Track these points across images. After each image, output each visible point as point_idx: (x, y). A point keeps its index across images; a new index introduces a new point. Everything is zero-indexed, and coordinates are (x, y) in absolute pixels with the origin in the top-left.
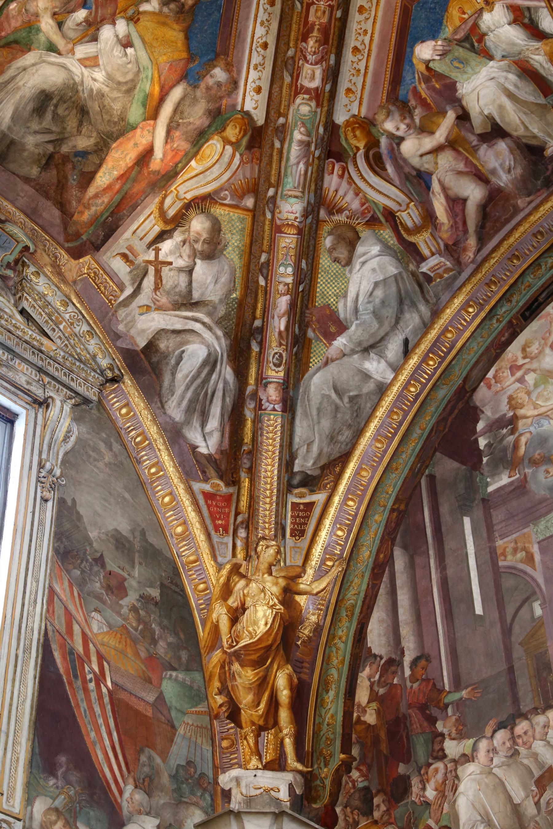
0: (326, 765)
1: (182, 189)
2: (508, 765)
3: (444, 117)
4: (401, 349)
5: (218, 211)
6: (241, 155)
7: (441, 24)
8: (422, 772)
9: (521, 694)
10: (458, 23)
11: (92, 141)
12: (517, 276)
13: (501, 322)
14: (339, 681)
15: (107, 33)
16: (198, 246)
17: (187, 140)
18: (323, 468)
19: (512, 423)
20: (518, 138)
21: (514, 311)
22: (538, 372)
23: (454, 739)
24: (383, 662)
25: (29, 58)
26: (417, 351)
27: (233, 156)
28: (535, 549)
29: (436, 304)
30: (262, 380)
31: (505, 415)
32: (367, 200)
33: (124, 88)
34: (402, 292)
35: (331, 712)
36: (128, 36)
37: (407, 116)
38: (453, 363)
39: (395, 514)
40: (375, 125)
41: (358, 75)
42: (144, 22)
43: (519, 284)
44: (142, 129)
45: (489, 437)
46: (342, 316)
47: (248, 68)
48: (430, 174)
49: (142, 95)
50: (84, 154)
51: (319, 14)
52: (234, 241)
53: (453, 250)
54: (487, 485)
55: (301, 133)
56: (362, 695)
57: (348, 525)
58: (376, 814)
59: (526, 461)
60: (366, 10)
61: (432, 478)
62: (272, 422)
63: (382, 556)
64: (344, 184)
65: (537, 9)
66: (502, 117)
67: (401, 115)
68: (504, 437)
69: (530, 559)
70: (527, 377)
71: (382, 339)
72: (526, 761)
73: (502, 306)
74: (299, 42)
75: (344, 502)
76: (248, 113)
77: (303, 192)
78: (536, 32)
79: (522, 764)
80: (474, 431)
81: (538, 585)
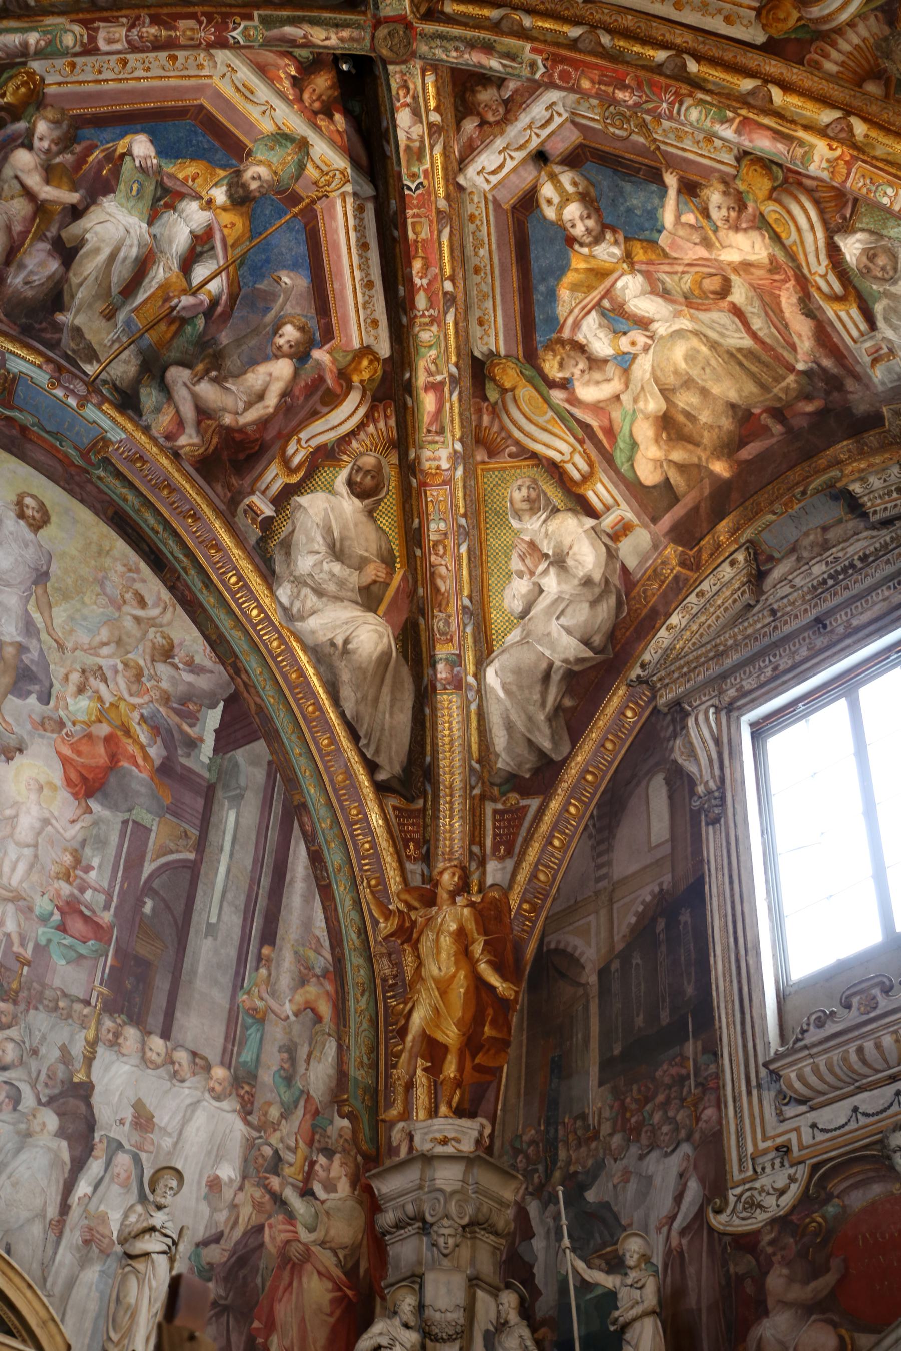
7: (177, 158)
10: (181, 176)
40: (37, 109)
51: (189, 33)
66: (87, 255)
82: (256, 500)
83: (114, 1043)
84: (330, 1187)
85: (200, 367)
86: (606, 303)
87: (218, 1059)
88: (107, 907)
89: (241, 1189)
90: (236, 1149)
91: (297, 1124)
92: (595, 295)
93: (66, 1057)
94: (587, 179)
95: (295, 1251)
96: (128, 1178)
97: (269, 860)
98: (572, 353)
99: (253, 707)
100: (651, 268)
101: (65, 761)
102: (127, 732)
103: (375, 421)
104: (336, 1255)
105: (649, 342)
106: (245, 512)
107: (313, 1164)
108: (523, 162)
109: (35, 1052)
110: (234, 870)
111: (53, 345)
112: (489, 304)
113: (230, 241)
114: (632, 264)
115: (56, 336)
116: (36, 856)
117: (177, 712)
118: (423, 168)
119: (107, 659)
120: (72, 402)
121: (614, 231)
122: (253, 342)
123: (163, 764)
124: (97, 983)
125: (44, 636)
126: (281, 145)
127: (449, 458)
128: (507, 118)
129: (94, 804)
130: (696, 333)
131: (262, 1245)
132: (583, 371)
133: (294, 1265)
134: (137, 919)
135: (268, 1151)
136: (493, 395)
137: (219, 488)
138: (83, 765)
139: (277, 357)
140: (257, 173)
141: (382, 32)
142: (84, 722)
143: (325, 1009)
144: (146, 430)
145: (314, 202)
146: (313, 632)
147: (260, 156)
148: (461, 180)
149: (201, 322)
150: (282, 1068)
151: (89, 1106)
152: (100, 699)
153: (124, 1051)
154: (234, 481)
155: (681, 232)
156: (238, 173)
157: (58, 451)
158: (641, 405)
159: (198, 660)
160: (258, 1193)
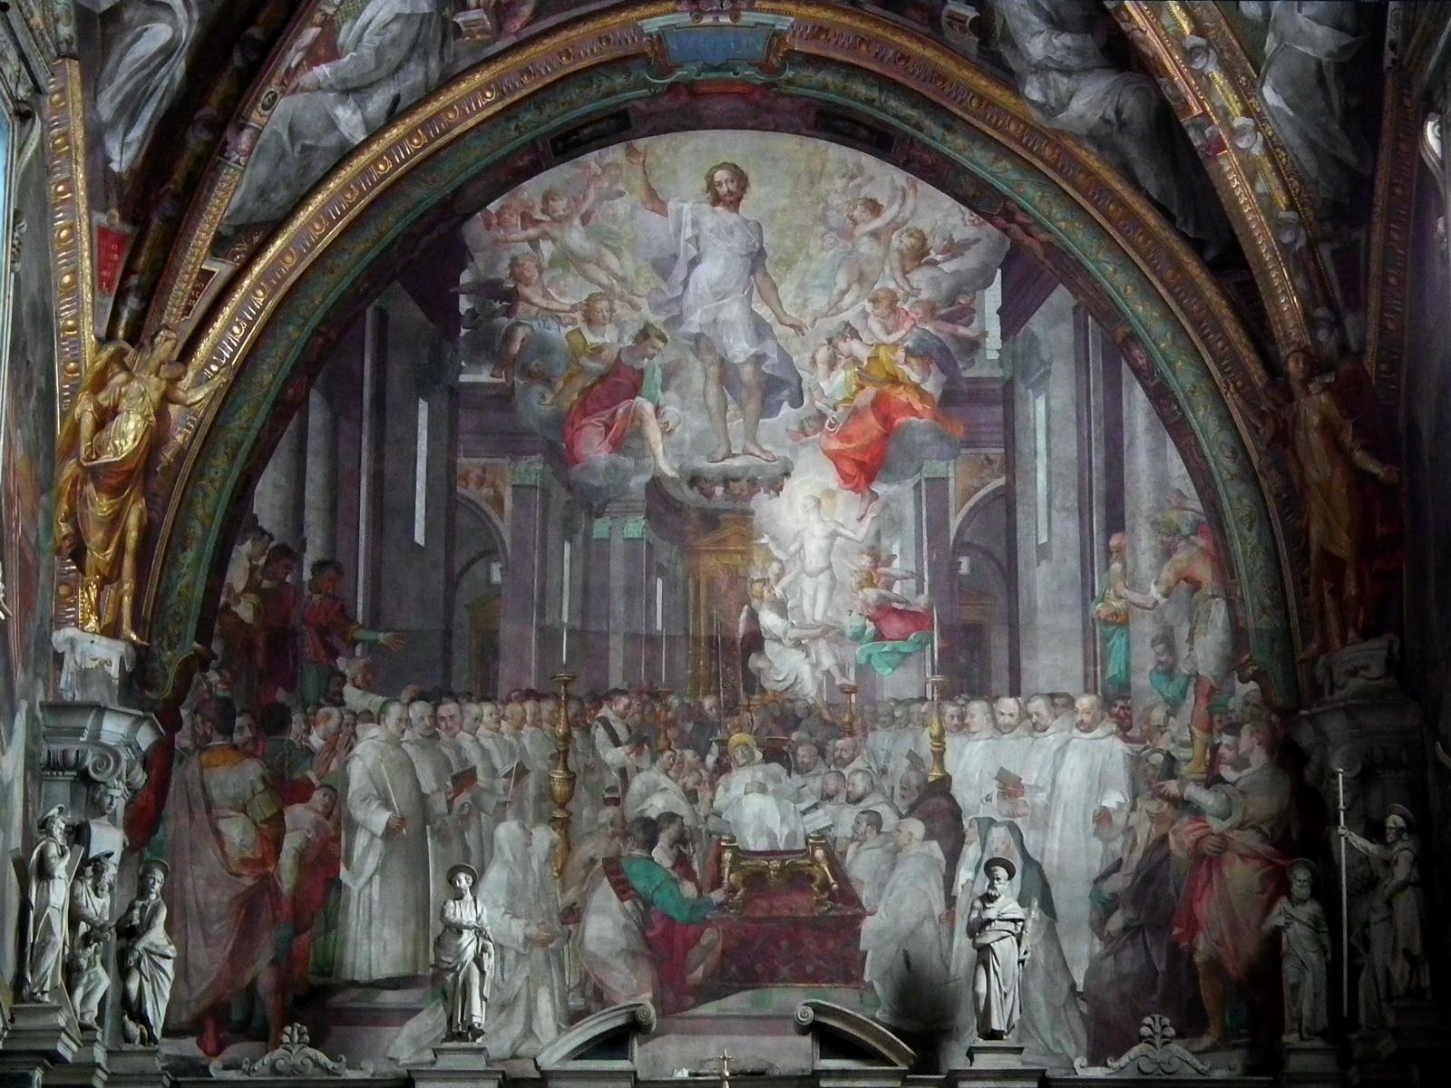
0: (171, 647)
2: (423, 747)
8: (309, 710)
9: (455, 668)
13: (521, 134)
14: (204, 540)
19: (512, 297)
21: (543, 129)
22: (558, 245)
23: (358, 687)
24: (273, 544)
28: (507, 493)
29: (450, 66)
35: (187, 579)
54: (460, 370)
56: (237, 576)
57: (247, 321)
58: (237, 737)
59: (518, 366)
61: (382, 316)
63: (290, 391)
68: (494, 314)
69: (498, 502)
72: (446, 751)
75: (252, 291)
79: (439, 750)
81: (502, 542)
83: (962, 726)
84: (1240, 763)
87: (1081, 689)
88: (919, 591)
89: (1133, 809)
90: (1120, 773)
91: (1189, 714)
93: (914, 757)
95: (1209, 846)
96: (1008, 847)
97: (1097, 431)
99: (1039, 250)
101: (835, 457)
102: (895, 380)
104: (1260, 830)
107: (1215, 749)
109: (884, 771)
110: (1054, 470)
116: (833, 578)
117: (950, 319)
119: (854, 307)
120: (725, 20)
123: (944, 394)
124: (928, 675)
125: (779, 329)
129: (880, 488)
131: (1168, 854)
133: (1211, 860)
134: (956, 586)
135: (1158, 758)
137: (912, 13)
138: (856, 450)
142: (845, 400)
143: (1204, 572)
150: (1159, 662)
151: (952, 799)
152: (856, 361)
153: (973, 729)
160: (1154, 806)
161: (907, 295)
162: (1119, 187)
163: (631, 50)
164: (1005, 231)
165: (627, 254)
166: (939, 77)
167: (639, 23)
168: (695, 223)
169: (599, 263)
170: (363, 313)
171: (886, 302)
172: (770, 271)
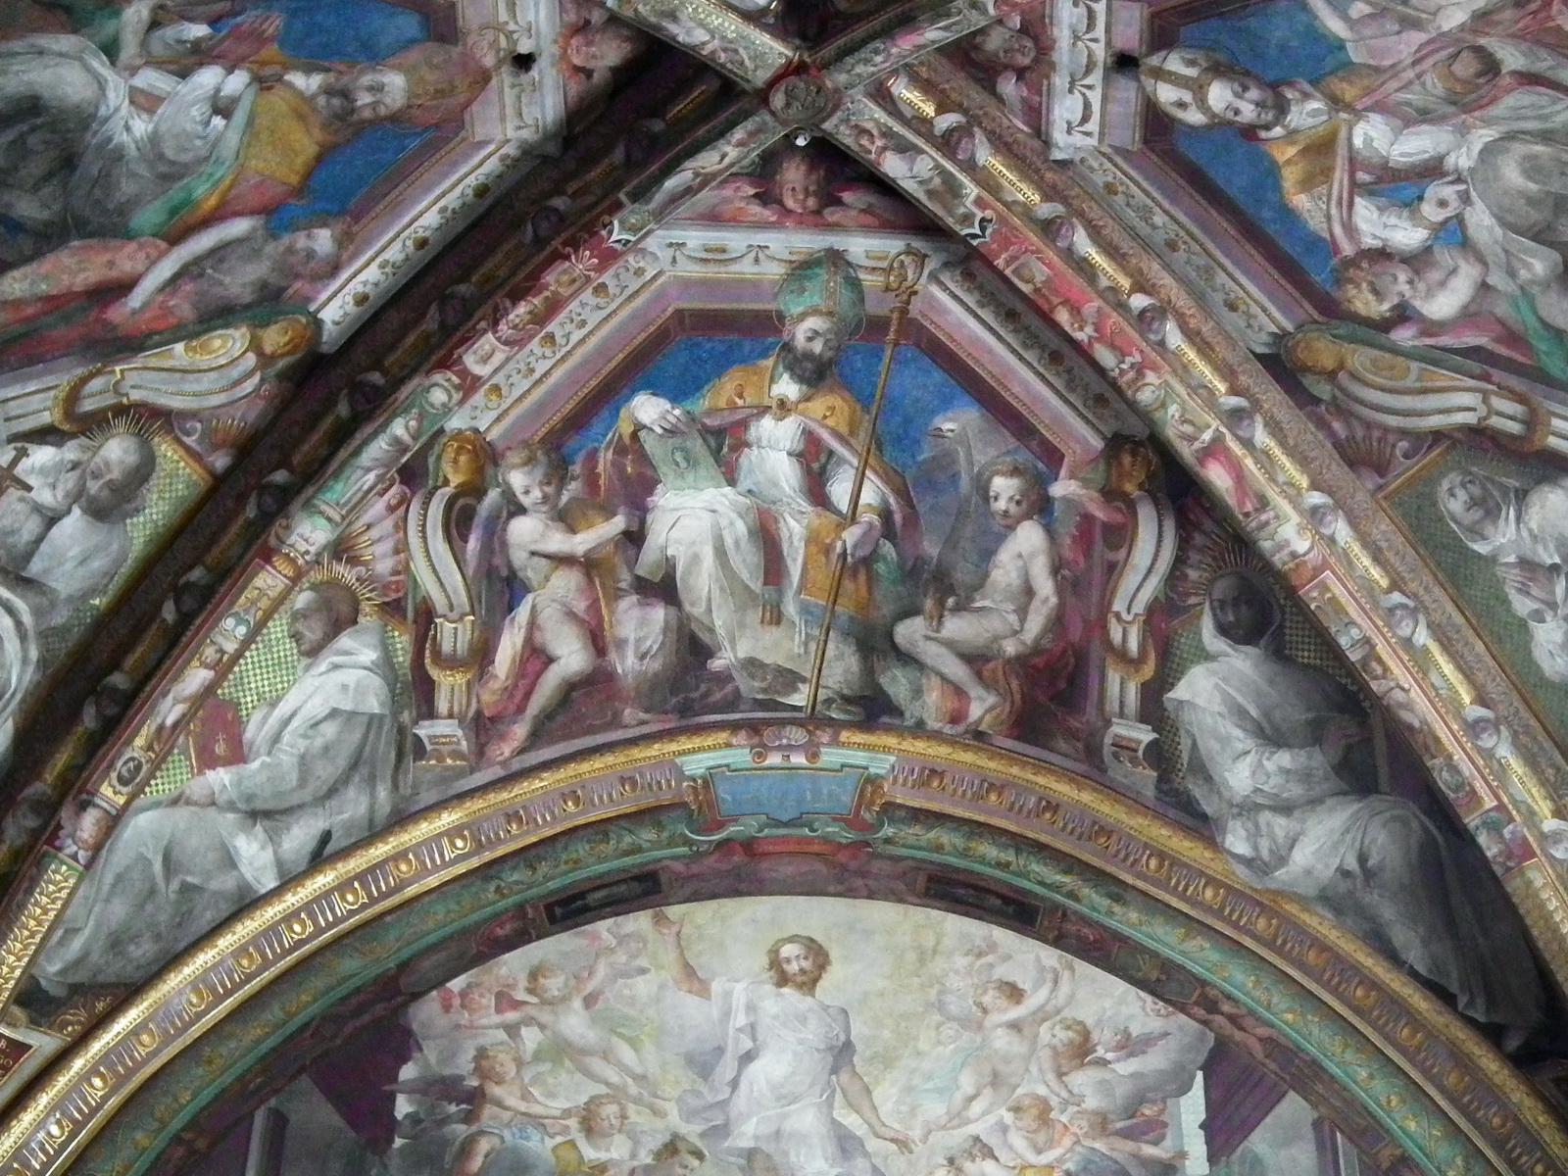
1: (133, 378)
3: (607, 519)
4: (311, 845)
5: (166, 450)
6: (262, 380)
7: (699, 388)
10: (722, 403)
11: (45, 215)
12: (559, 829)
13: (504, 896)
15: (208, 78)
16: (93, 487)
17: (195, 306)
18: (75, 989)
19: (475, 1099)
20: (689, 617)
21: (534, 891)
22: (548, 1033)
25: (66, 42)
26: (340, 865)
27: (250, 374)
29: (407, 799)
30: (80, 792)
31: (462, 1078)
32: (407, 568)
33: (163, 168)
34: (368, 749)
36: (234, 101)
37: (555, 481)
38: (388, 919)
39: (180, 1151)
40: (496, 464)
41: (525, 377)
42: (277, 100)
43: (559, 846)
44: (141, 247)
45: (420, 1103)
46: (249, 733)
47: (373, 259)
48: (527, 589)
49: (182, 195)
50: (16, 227)
51: (565, 278)
52: (156, 510)
53: (483, 727)
55: (407, 428)
57: (75, 1122)
60: (607, 295)
61: (279, 1123)
62: (58, 877)
64: (388, 524)
65: (842, 461)
66: (688, 572)
67: (546, 475)
68: (446, 1120)
70: (524, 1031)
71: (289, 811)
73: (514, 868)
74: (502, 292)
75: (85, 1077)
76: (318, 324)
77: (343, 518)
78: (816, 489)
80: (394, 1079)
82: (1120, 729)
85: (929, 604)
86: (1363, 177)
92: (1340, 176)
94: (1200, 47)
98: (1377, 268)
100: (1377, 96)
103: (1197, 526)
105: (1462, 187)
106: (1116, 756)
108: (1106, 79)
111: (733, 702)
112: (1221, 278)
113: (844, 429)
114: (1349, 107)
115: (729, 688)
117: (1127, 1134)
118: (969, 202)
120: (799, 759)
121: (1291, 84)
122: (968, 531)
125: (872, 1144)
126: (810, 279)
127: (1301, 529)
128: (1044, 49)
130: (1511, 137)
132: (1411, 282)
136: (1323, 390)
137: (1062, 745)
139: (1012, 528)
140: (808, 331)
141: (778, 100)
144: (919, 730)
145: (904, 311)
146: (1308, 872)
147: (796, 310)
148: (1057, 155)
149: (887, 548)
154: (1074, 724)
155: (1368, 32)
156: (788, 348)
157: (809, 841)
158: (1524, 274)
159: (1135, 1030)
161: (1065, 1103)
162: (1369, 962)
163: (666, 798)
164: (1205, 1023)
165: (648, 1046)
166: (1103, 830)
167: (677, 760)
168: (751, 1008)
169: (606, 1055)
170: (251, 1115)
171: (1034, 1112)
172: (858, 1069)
